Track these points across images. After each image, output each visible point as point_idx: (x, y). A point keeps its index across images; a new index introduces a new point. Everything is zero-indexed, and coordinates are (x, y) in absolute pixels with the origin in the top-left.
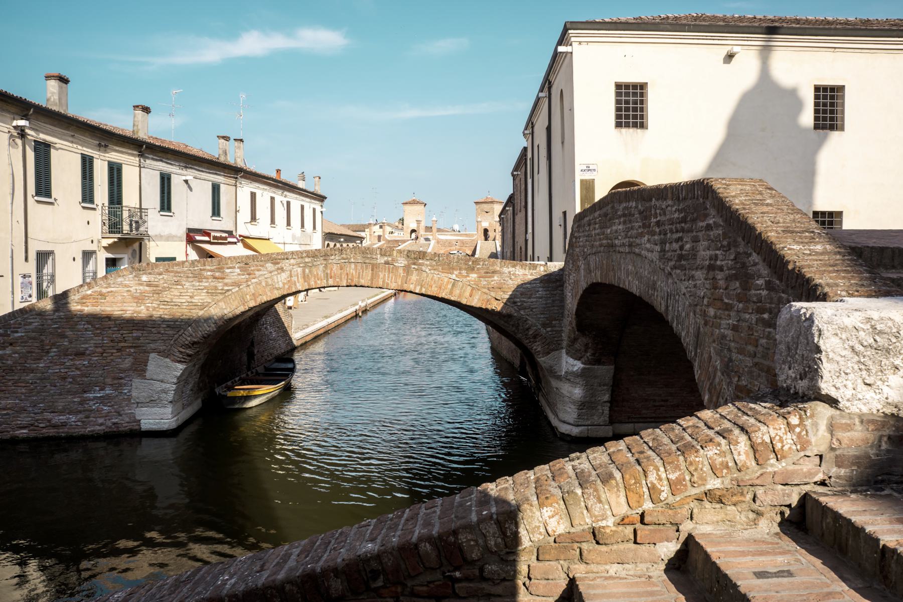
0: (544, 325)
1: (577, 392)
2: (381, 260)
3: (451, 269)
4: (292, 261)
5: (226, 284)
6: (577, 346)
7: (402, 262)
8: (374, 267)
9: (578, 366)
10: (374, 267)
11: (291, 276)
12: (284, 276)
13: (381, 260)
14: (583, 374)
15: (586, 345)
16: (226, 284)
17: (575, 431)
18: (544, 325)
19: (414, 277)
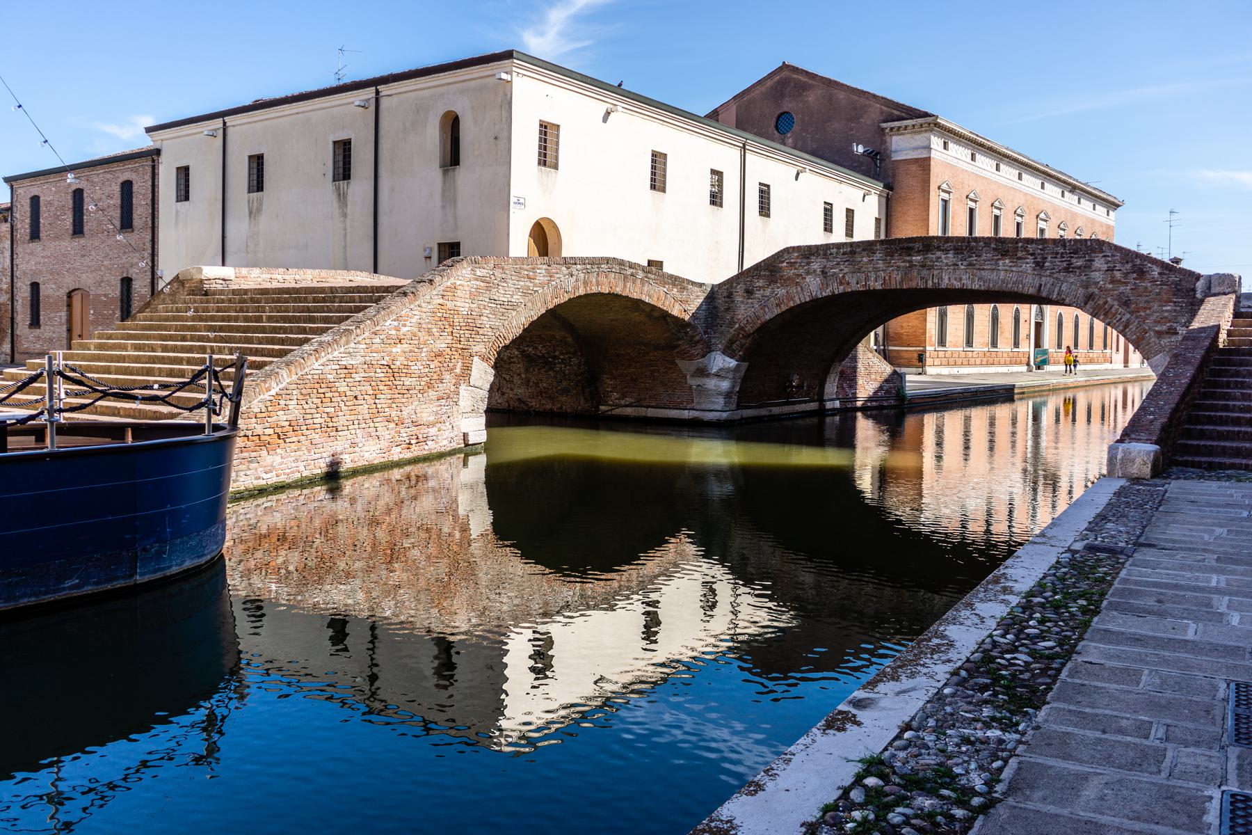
0: (706, 333)
1: (725, 385)
2: (629, 271)
3: (664, 284)
4: (579, 267)
5: (535, 286)
6: (734, 347)
7: (641, 275)
8: (626, 277)
9: (732, 363)
10: (626, 277)
11: (577, 281)
12: (573, 280)
13: (629, 271)
14: (737, 369)
15: (742, 346)
16: (535, 286)
17: (725, 415)
18: (706, 333)
19: (646, 288)
